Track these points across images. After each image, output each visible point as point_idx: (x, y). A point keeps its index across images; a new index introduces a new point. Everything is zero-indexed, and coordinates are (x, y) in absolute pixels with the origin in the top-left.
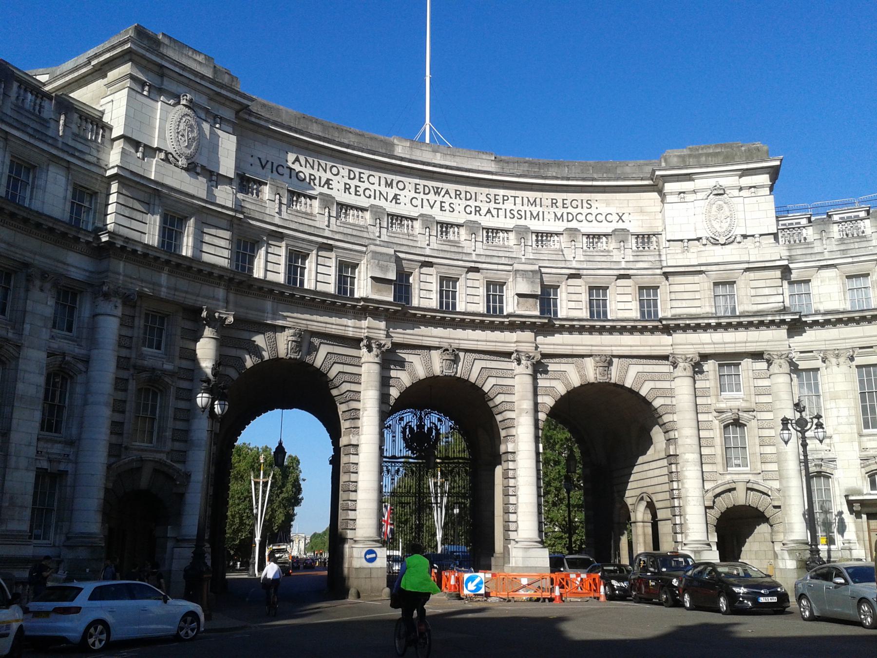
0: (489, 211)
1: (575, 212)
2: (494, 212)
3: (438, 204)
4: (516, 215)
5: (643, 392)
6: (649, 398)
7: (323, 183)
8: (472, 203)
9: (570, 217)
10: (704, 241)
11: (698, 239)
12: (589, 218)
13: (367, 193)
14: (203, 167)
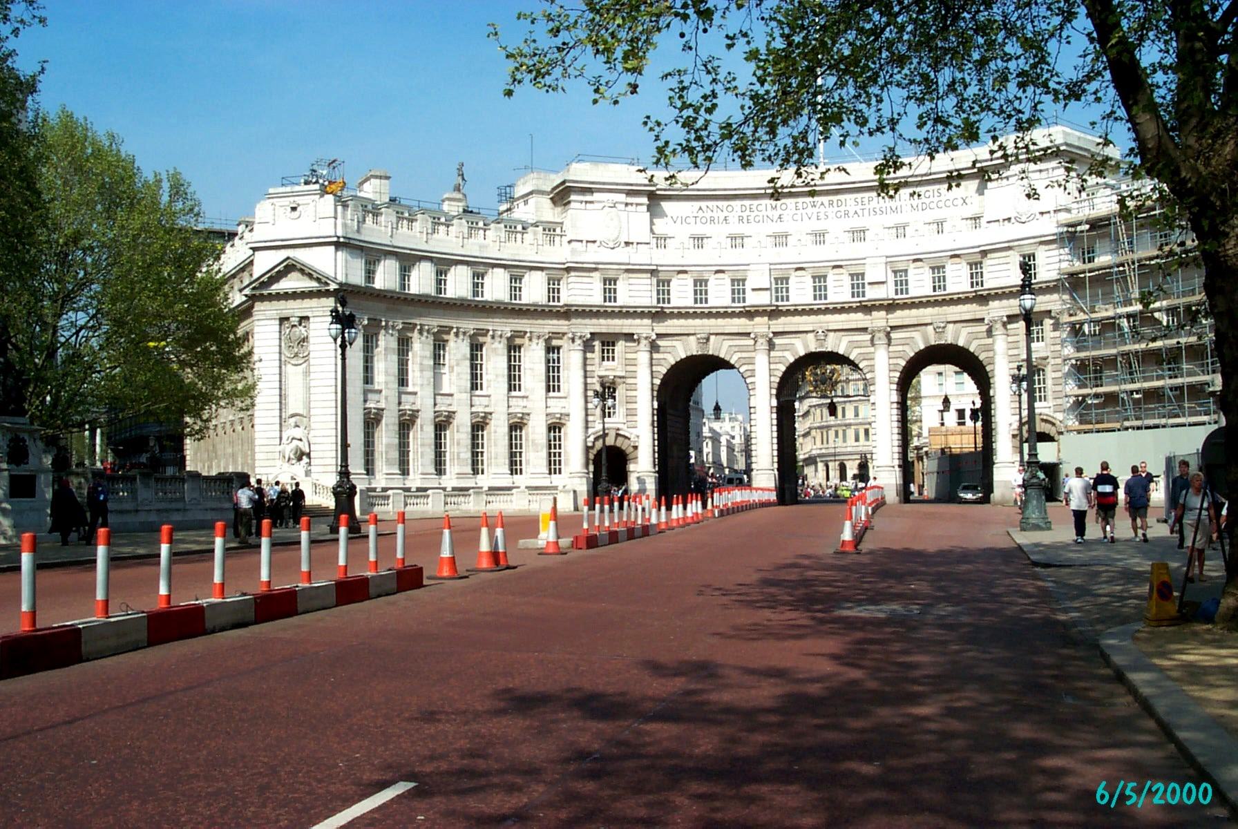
0: (856, 213)
1: (927, 201)
2: (860, 212)
3: (815, 217)
4: (879, 212)
5: (972, 350)
6: (976, 354)
7: (722, 219)
8: (843, 208)
9: (924, 206)
10: (1013, 220)
11: (1009, 219)
12: (940, 204)
13: (757, 219)
14: (627, 244)
